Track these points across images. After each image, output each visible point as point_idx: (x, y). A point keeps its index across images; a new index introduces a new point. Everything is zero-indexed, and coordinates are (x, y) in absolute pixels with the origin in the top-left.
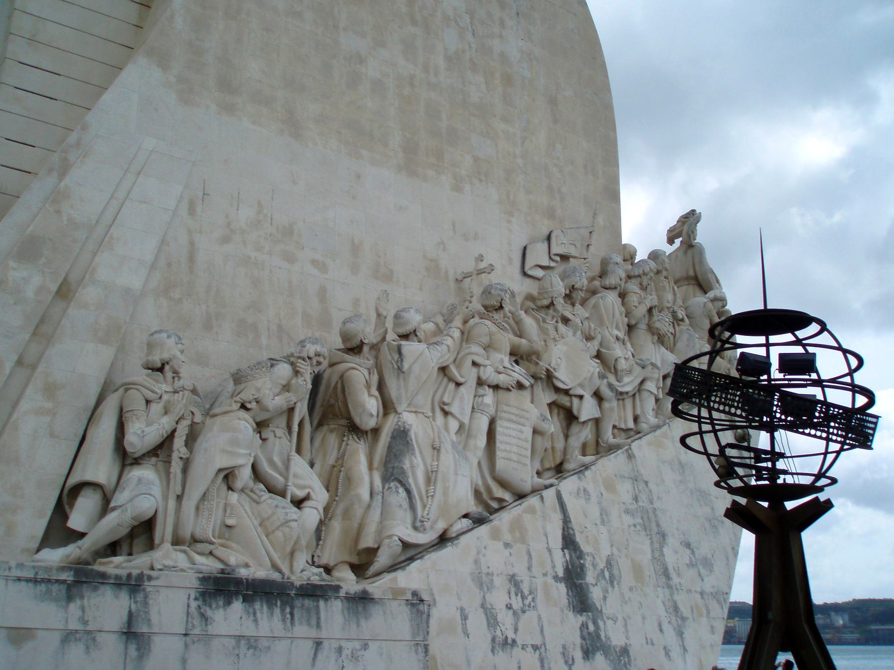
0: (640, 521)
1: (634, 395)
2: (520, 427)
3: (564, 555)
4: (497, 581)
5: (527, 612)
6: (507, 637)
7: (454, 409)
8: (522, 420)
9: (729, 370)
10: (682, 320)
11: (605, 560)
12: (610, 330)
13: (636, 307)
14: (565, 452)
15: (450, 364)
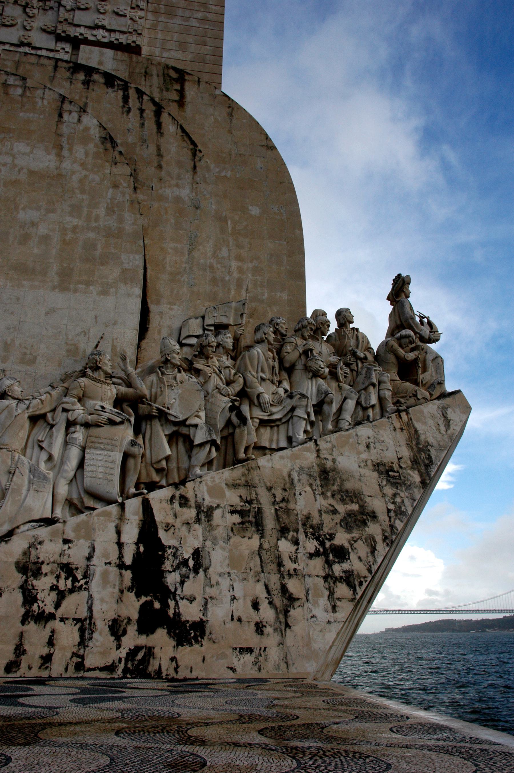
0: (251, 519)
1: (288, 421)
2: (106, 452)
3: (138, 548)
4: (45, 569)
5: (75, 594)
6: (44, 611)
7: (44, 445)
8: (110, 447)
9: (416, 391)
10: (366, 358)
11: (191, 551)
12: (254, 374)
13: (289, 353)
14: (189, 470)
15: (50, 412)
